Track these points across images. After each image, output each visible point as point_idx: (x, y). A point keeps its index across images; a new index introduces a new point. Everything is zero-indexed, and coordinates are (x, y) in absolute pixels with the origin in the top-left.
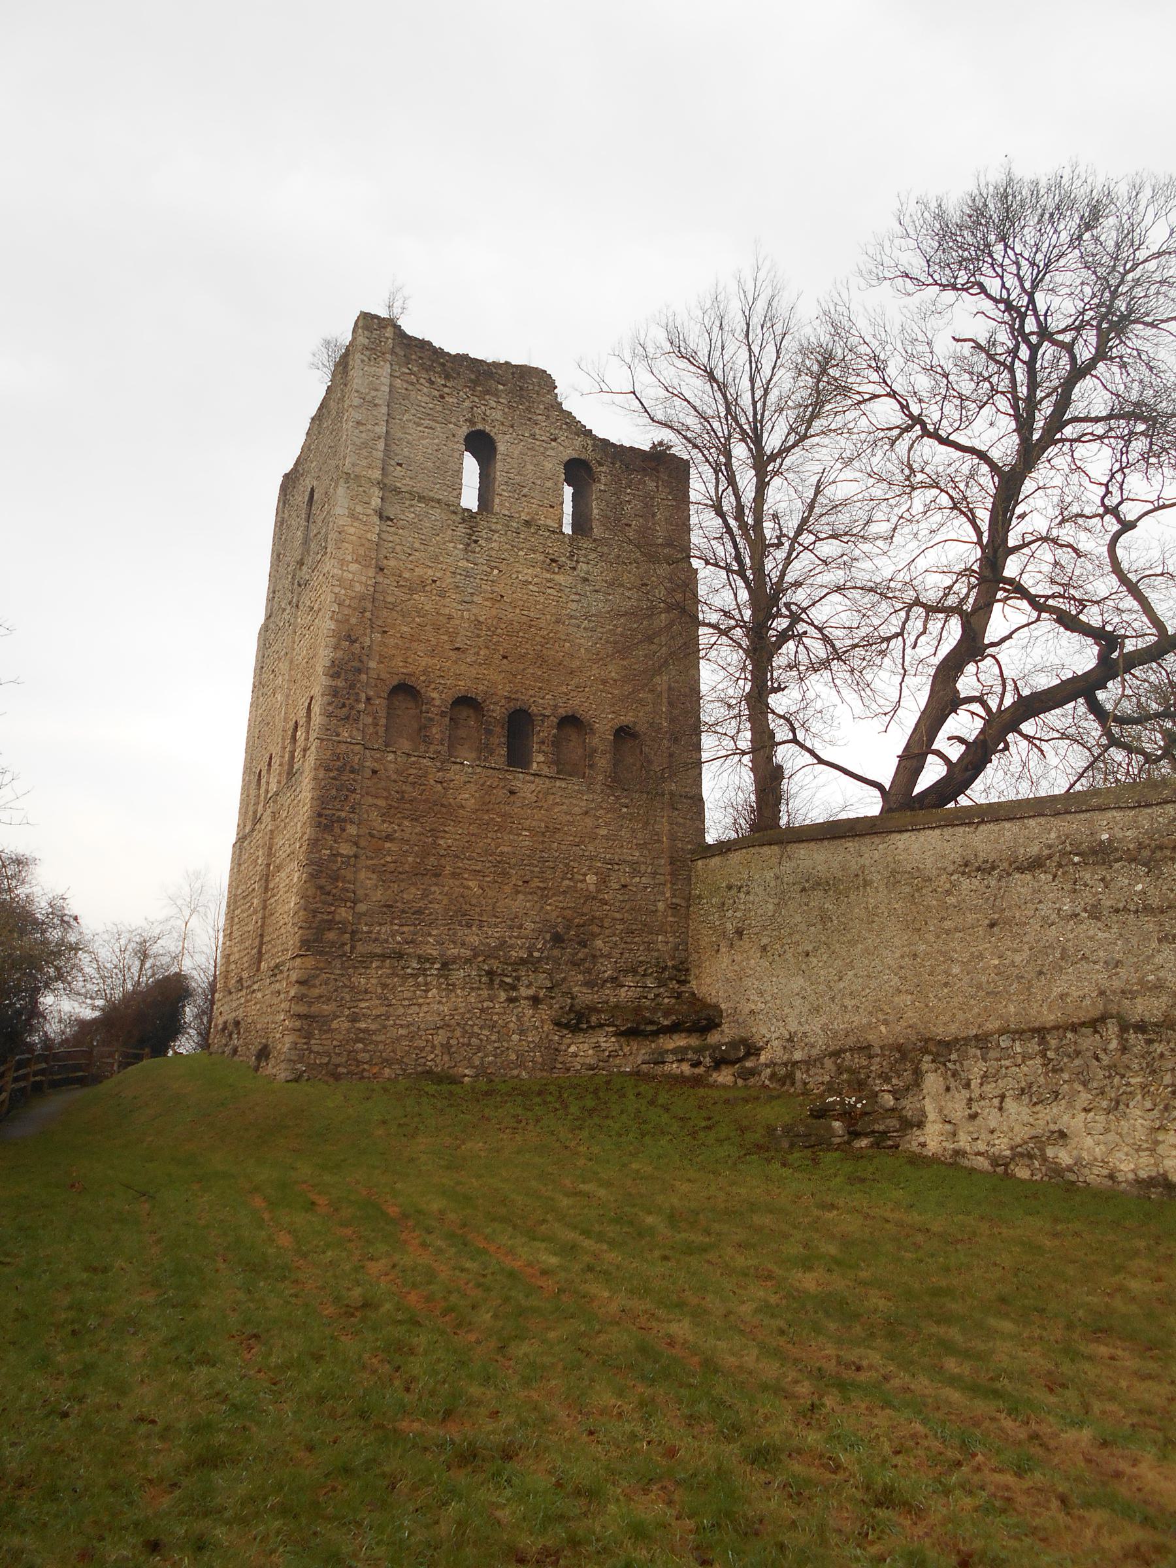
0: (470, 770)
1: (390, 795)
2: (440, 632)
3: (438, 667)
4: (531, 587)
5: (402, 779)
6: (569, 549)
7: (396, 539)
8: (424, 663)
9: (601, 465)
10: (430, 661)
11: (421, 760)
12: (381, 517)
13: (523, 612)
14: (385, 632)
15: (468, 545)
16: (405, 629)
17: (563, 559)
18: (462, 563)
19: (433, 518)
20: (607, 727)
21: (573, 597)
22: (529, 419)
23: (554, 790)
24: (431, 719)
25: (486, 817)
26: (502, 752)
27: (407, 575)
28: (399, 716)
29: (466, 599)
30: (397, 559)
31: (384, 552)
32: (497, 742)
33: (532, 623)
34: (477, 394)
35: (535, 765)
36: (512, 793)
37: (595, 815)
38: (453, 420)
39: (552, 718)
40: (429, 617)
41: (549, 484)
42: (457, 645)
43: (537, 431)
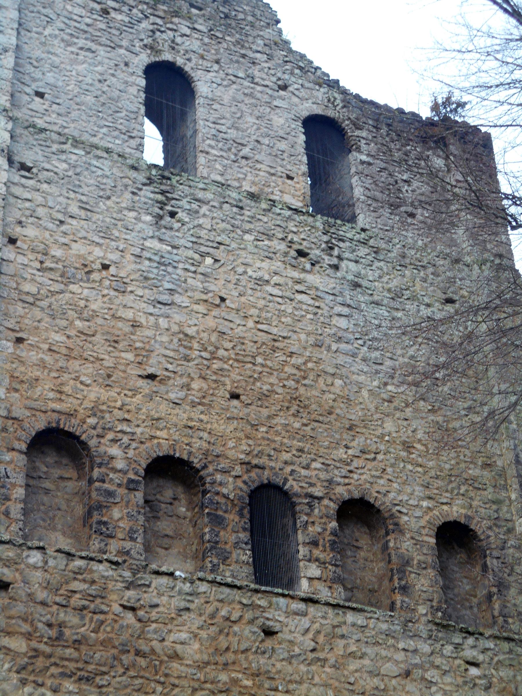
0: (187, 587)
1: (36, 630)
2: (120, 346)
3: (119, 404)
4: (269, 289)
5: (58, 599)
6: (325, 238)
7: (39, 198)
8: (92, 396)
9: (359, 128)
10: (104, 394)
11: (95, 566)
12: (10, 161)
13: (260, 326)
14: (19, 340)
15: (160, 217)
16: (59, 337)
17: (317, 252)
18: (154, 244)
19: (100, 172)
20: (423, 523)
21: (339, 309)
22: (244, 56)
23: (344, 630)
24: (110, 494)
25: (223, 677)
26: (244, 558)
27: (58, 252)
28: (47, 492)
29: (164, 298)
30: (39, 226)
31: (18, 214)
32: (233, 538)
33: (277, 344)
34: (161, 14)
35: (304, 584)
36: (269, 633)
37: (423, 679)
38: (124, 43)
39: (326, 502)
40: (100, 321)
41: (283, 145)
42: (151, 370)
43: (257, 73)
